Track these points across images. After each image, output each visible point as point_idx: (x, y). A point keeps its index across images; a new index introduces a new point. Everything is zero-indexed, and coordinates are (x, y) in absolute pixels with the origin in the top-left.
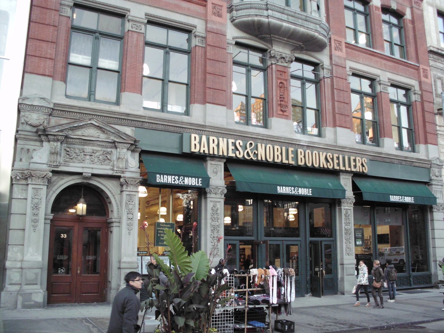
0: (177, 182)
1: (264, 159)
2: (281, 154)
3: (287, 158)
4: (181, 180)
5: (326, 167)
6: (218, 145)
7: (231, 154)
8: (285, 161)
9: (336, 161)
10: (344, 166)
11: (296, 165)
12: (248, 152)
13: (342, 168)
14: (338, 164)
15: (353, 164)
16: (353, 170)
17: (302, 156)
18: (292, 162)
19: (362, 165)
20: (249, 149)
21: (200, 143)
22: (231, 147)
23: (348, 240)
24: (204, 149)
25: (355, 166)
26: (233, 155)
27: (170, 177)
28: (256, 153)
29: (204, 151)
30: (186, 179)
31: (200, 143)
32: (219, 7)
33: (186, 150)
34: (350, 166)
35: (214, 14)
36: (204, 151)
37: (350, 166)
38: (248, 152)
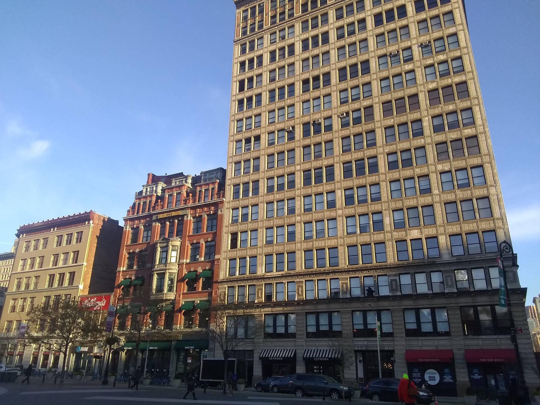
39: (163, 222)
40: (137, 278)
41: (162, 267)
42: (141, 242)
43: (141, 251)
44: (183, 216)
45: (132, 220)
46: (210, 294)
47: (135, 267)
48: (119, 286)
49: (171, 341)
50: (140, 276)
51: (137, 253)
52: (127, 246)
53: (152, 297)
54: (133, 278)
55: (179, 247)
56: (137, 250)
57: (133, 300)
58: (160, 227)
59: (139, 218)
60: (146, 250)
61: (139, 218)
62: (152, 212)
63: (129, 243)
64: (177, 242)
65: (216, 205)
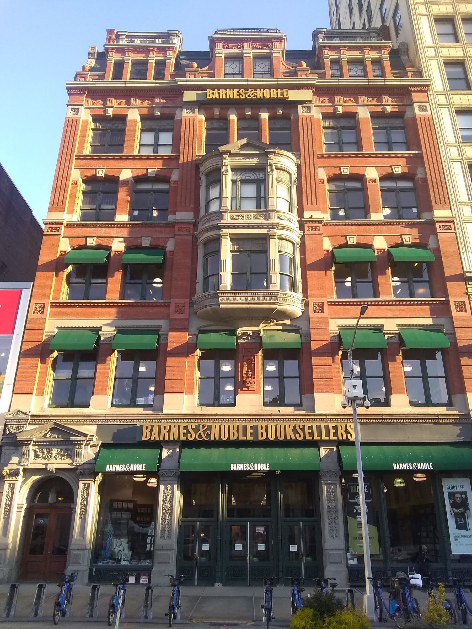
0: (123, 470)
1: (217, 438)
2: (238, 431)
3: (245, 434)
4: (127, 467)
5: (293, 438)
6: (169, 432)
7: (182, 438)
8: (242, 438)
9: (308, 431)
10: (320, 434)
11: (256, 440)
12: (200, 434)
13: (316, 438)
14: (311, 434)
15: (332, 431)
16: (333, 438)
17: (263, 431)
18: (250, 438)
19: (347, 432)
20: (201, 431)
21: (151, 431)
22: (182, 431)
23: (333, 521)
24: (155, 436)
25: (336, 434)
26: (185, 438)
27: (118, 466)
28: (209, 433)
29: (155, 438)
30: (132, 466)
31: (151, 431)
32: (181, 305)
33: (137, 440)
34: (328, 434)
35: (176, 312)
36: (155, 438)
37: (328, 434)
38: (200, 434)
39: (217, 112)
40: (130, 249)
41: (249, 216)
42: (136, 153)
43: (138, 180)
44: (296, 103)
45: (93, 93)
46: (442, 310)
47: (122, 217)
48: (58, 265)
49: (315, 444)
50: (146, 242)
51: (126, 182)
52: (79, 158)
53: (225, 303)
54: (118, 246)
55: (294, 178)
56: (126, 174)
57: (123, 311)
58: (204, 125)
59: (126, 95)
60: (160, 178)
61: (126, 95)
62: (181, 82)
63: (87, 151)
64: (286, 160)
65: (402, 93)
